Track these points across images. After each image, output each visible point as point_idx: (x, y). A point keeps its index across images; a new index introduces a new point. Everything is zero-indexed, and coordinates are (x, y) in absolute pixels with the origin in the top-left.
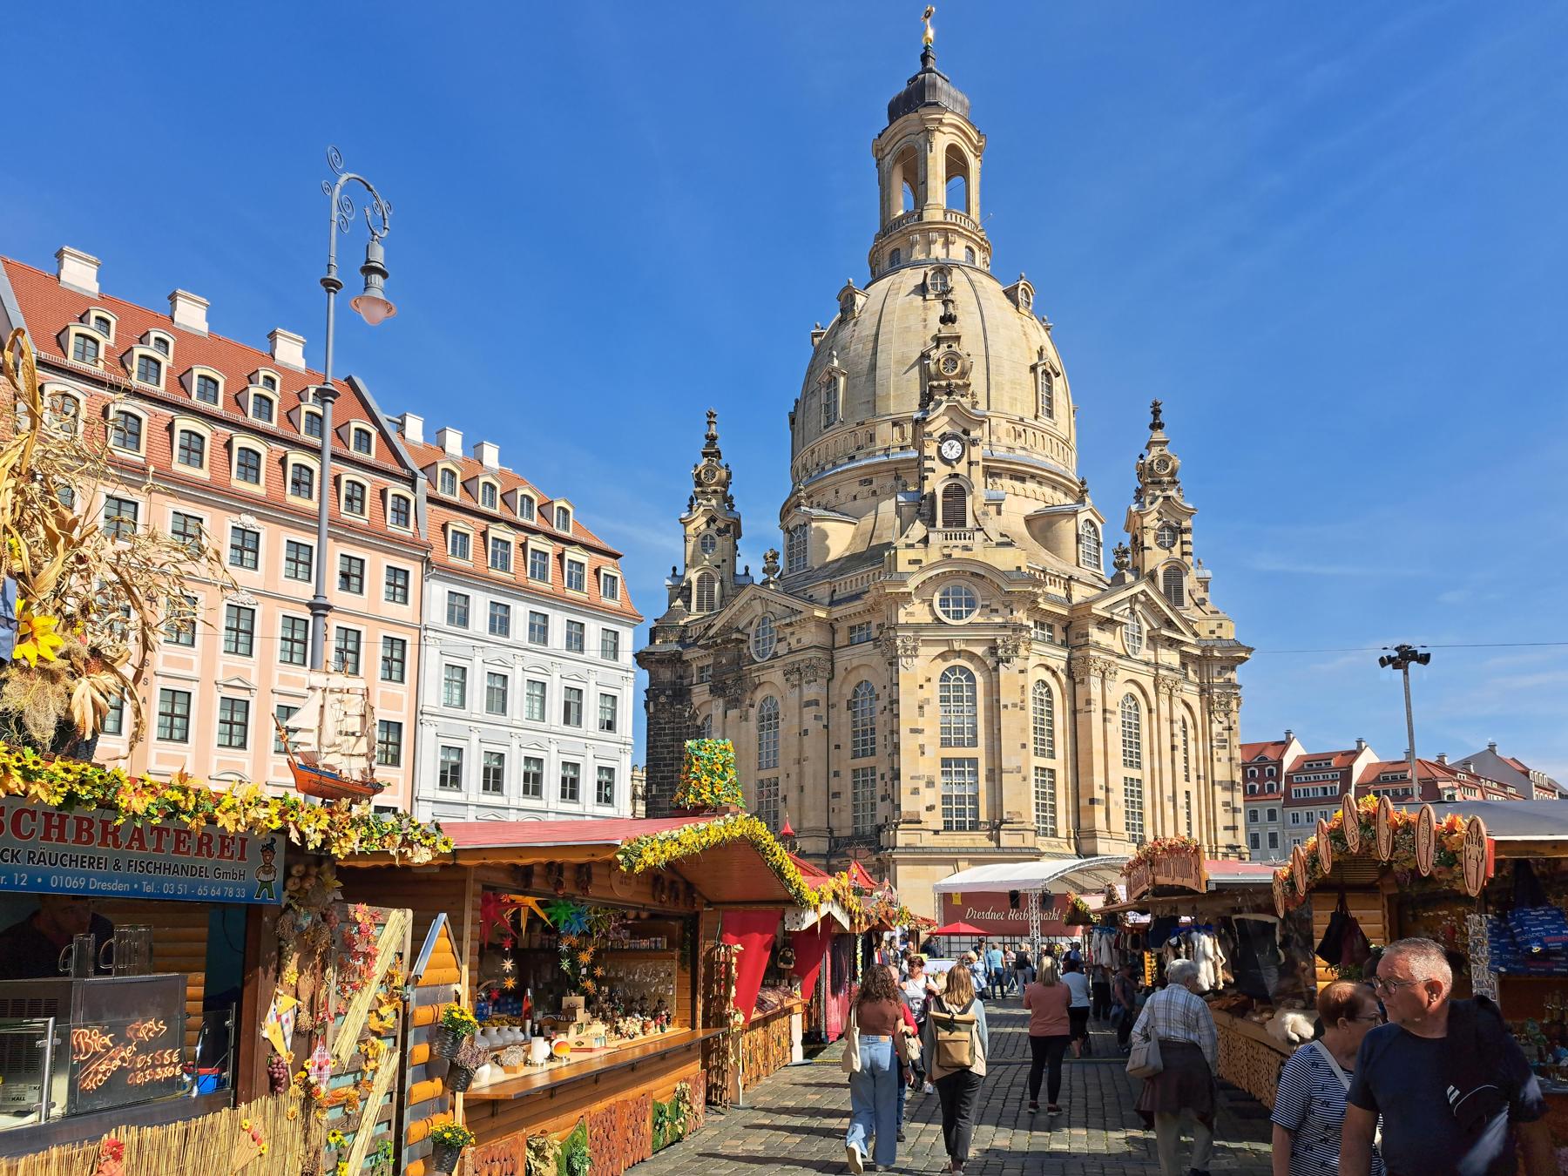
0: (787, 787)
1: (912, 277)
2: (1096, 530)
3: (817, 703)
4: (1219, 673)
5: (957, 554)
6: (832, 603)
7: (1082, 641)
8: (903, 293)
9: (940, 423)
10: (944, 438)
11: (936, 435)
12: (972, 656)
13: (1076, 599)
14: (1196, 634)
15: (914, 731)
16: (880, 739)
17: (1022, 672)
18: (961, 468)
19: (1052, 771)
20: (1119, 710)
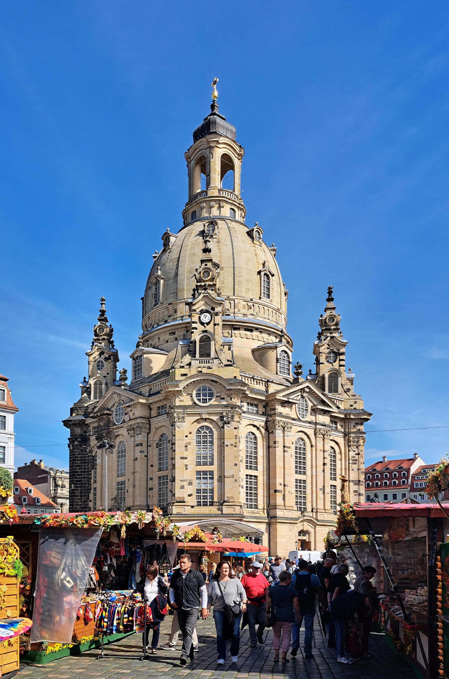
0: (128, 486)
1: (198, 226)
2: (288, 356)
3: (141, 444)
5: (205, 371)
6: (150, 395)
8: (193, 235)
9: (200, 305)
10: (202, 312)
12: (212, 421)
13: (271, 391)
15: (182, 458)
16: (170, 462)
17: (236, 428)
18: (210, 328)
19: (256, 477)
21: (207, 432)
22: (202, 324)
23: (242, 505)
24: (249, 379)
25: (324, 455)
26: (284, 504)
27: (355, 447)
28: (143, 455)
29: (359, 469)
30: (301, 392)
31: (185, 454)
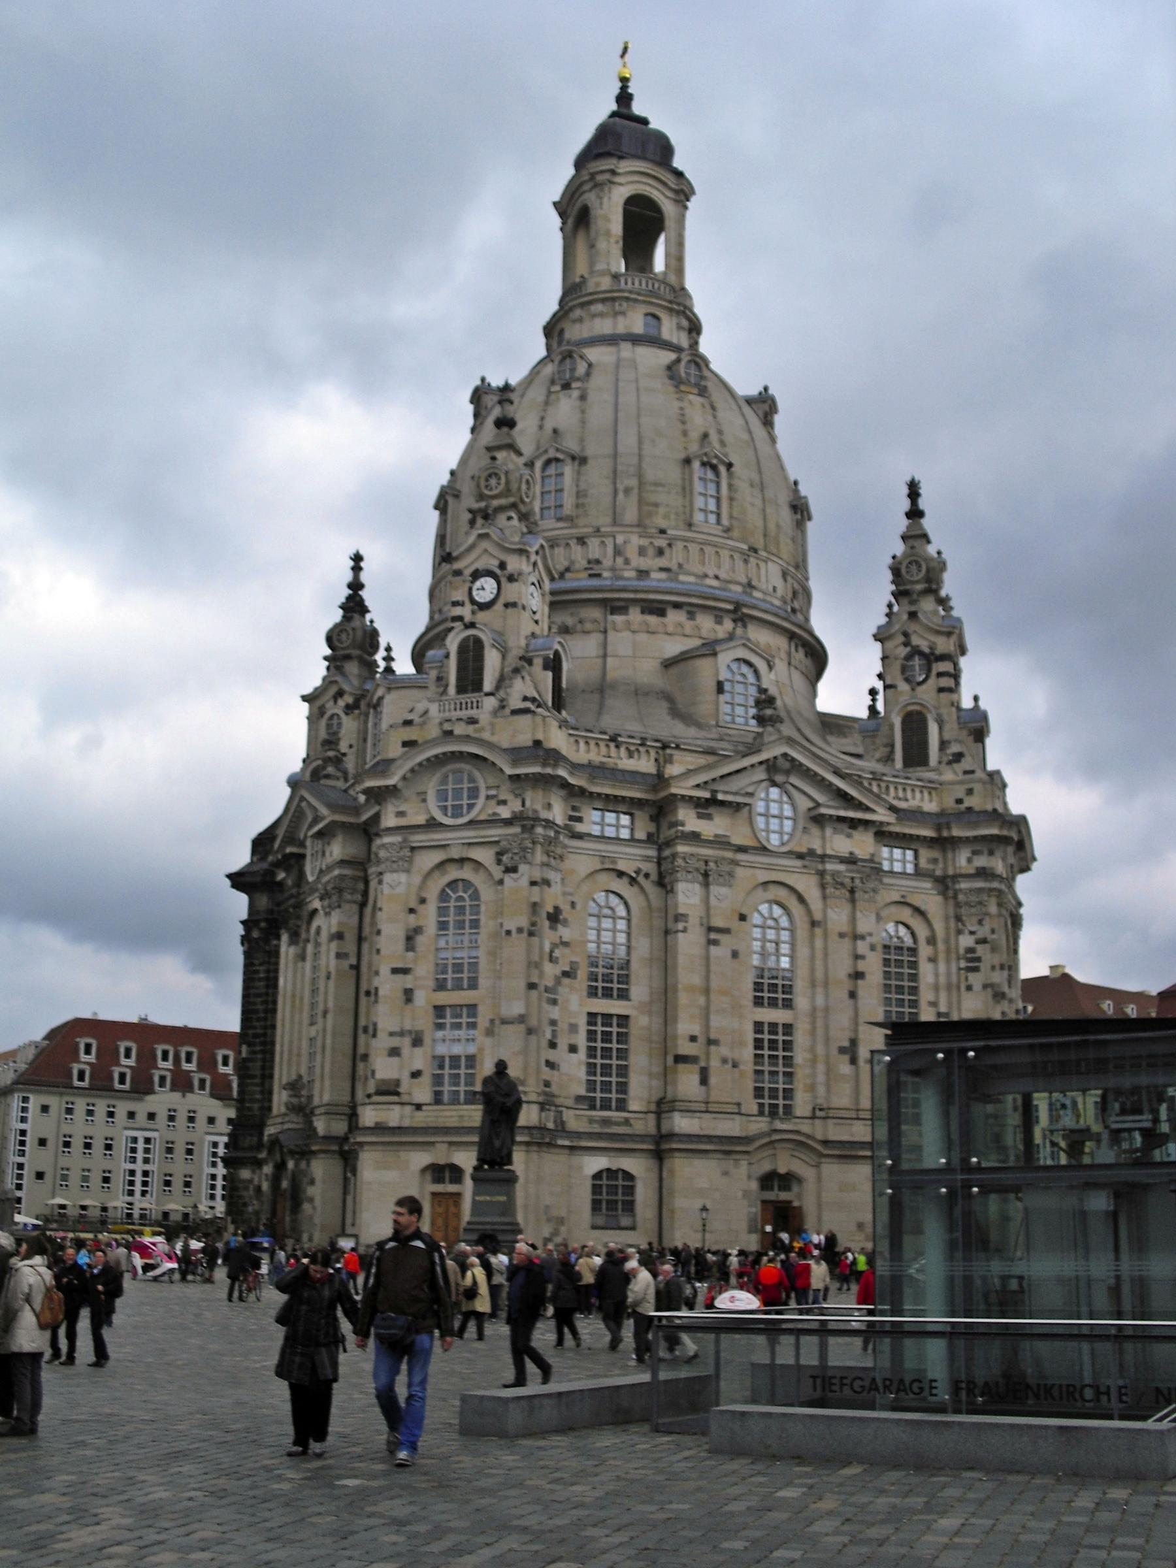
4: (969, 860)
5: (459, 729)
12: (477, 864)
13: (673, 770)
14: (892, 809)
15: (395, 971)
17: (533, 883)
19: (624, 1020)
21: (465, 895)
22: (473, 601)
23: (558, 1101)
24: (602, 744)
25: (855, 948)
26: (708, 1094)
27: (975, 920)
28: (346, 964)
29: (985, 986)
30: (768, 770)
31: (409, 959)
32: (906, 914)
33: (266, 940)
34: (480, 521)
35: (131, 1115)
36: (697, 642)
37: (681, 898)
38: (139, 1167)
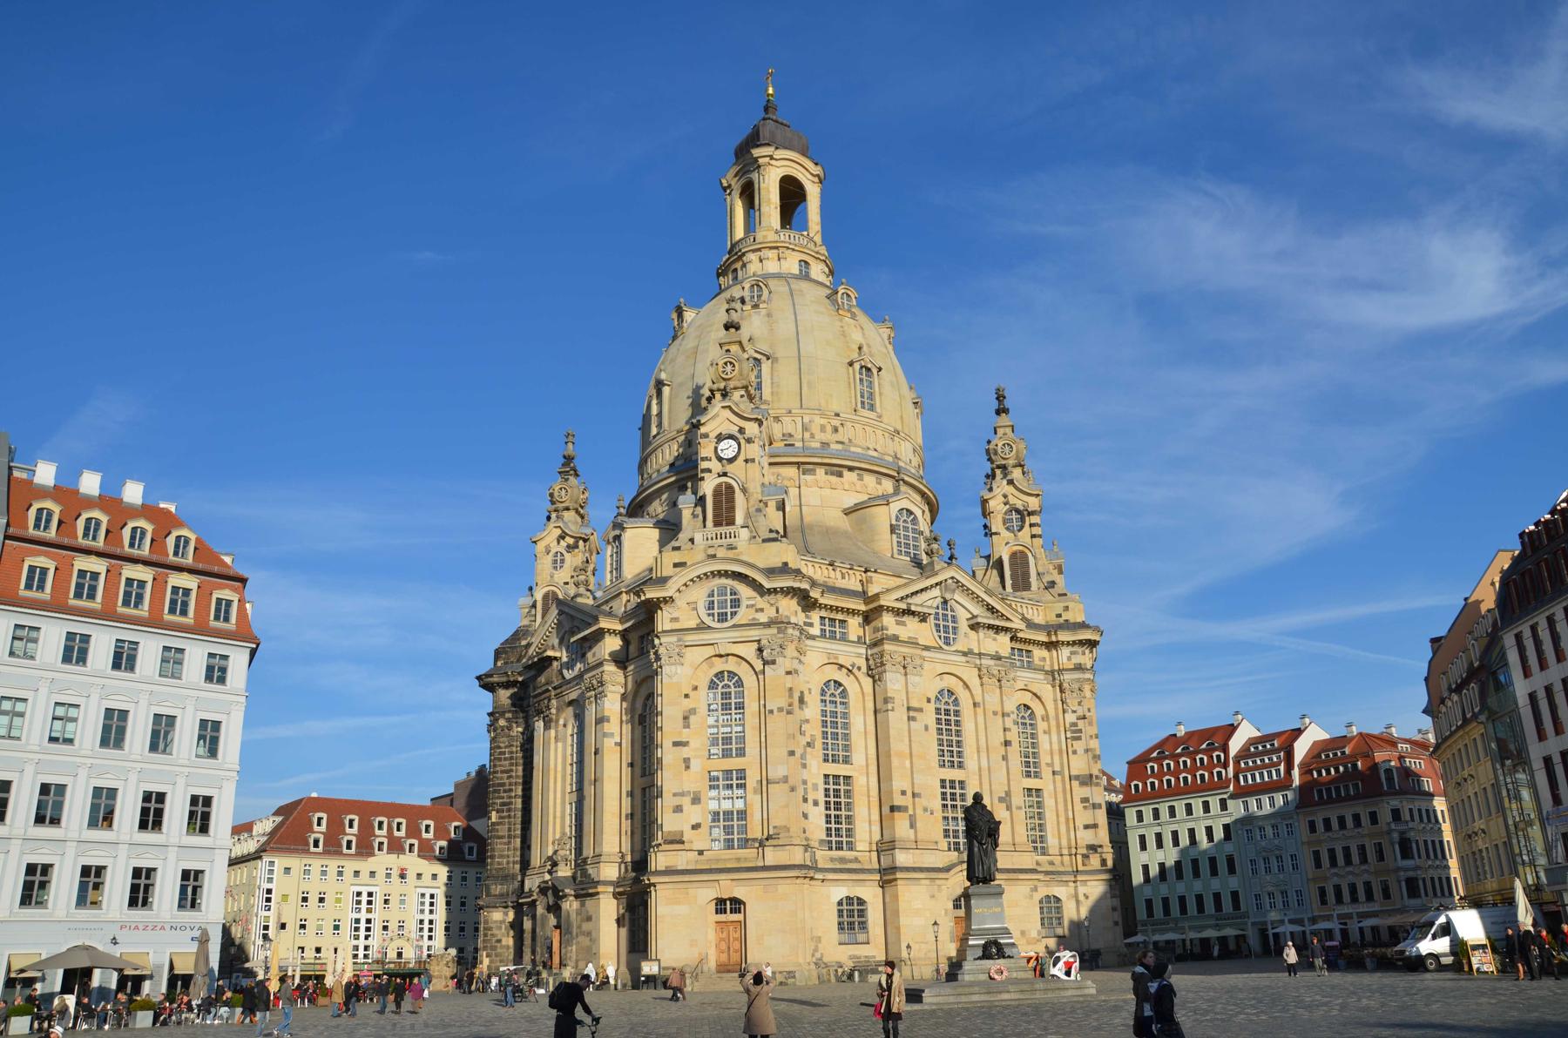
4: (1069, 659)
5: (721, 553)
7: (879, 635)
11: (713, 435)
14: (1024, 619)
15: (676, 744)
17: (789, 673)
19: (847, 778)
20: (932, 706)
22: (720, 459)
23: (813, 844)
29: (1087, 751)
32: (1027, 699)
33: (510, 728)
34: (718, 396)
35: (357, 873)
36: (866, 497)
37: (889, 685)
38: (363, 916)
